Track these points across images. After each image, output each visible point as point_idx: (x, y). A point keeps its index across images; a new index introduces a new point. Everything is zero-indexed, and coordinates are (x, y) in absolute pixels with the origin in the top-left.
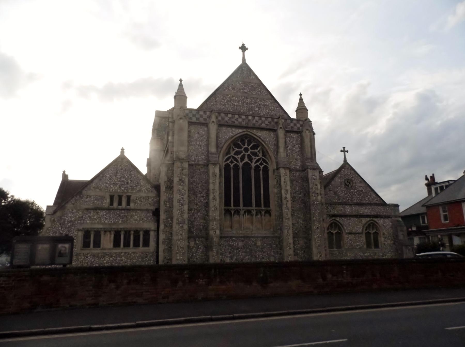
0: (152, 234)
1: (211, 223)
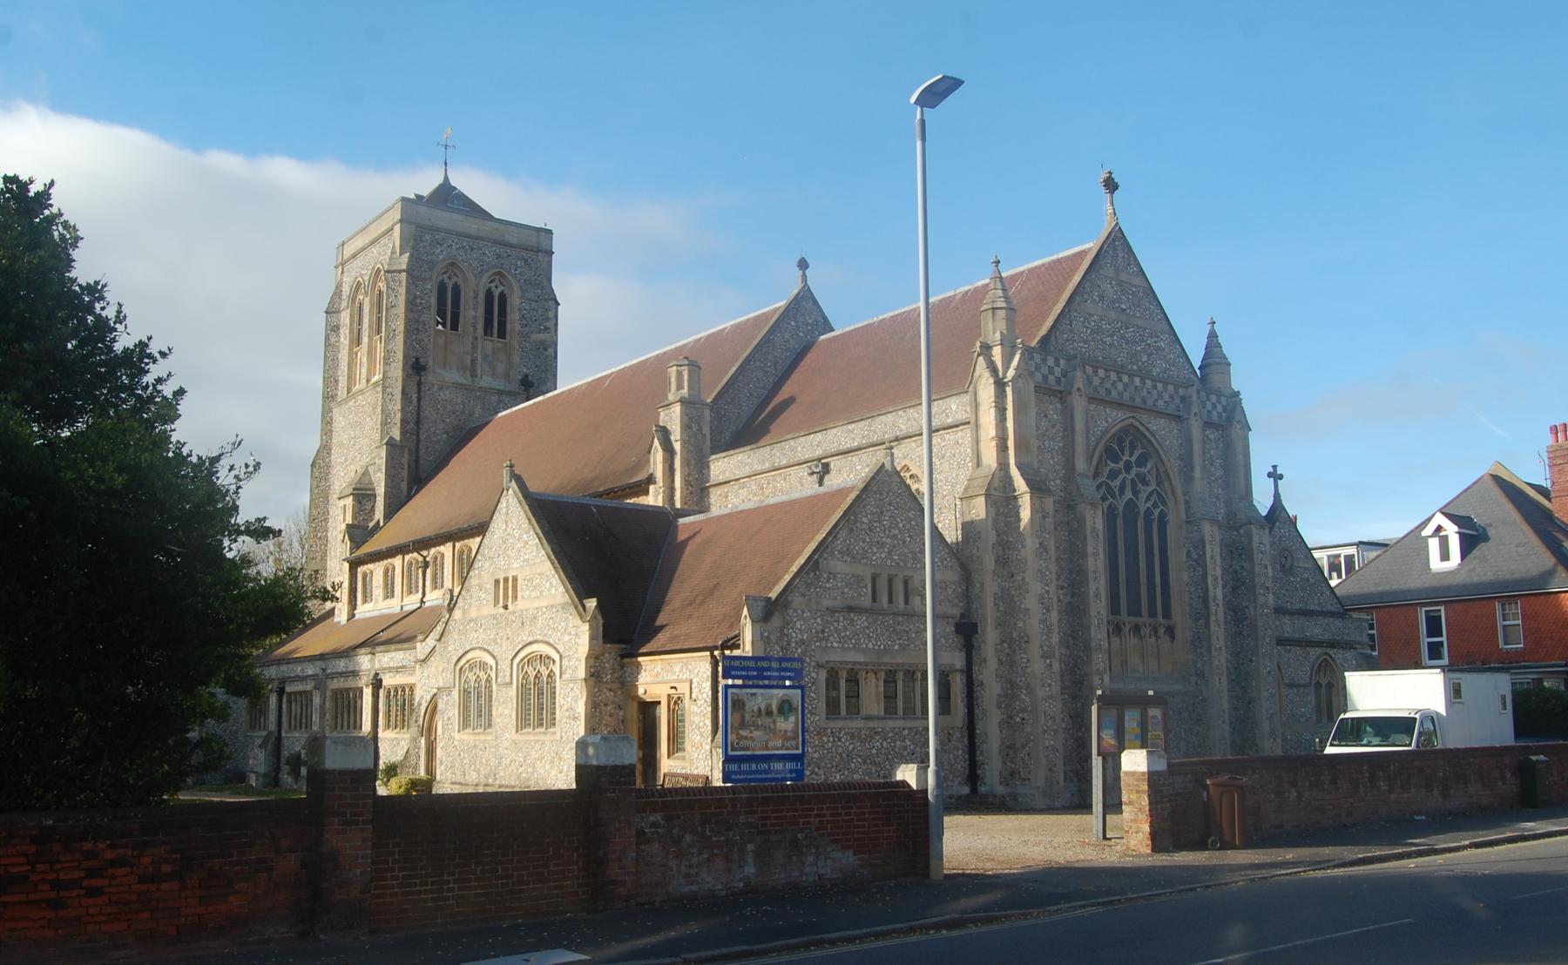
1: (1094, 657)
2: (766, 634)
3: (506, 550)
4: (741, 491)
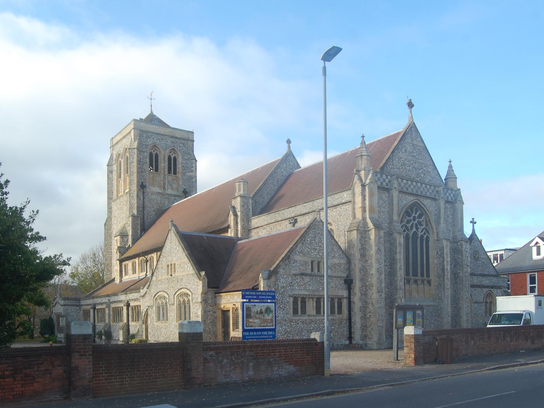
0: (345, 302)
1: (399, 292)
2: (269, 284)
3: (171, 253)
4: (264, 230)
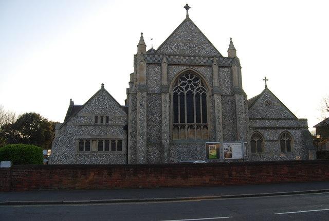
0: (124, 143)
1: (163, 135)
